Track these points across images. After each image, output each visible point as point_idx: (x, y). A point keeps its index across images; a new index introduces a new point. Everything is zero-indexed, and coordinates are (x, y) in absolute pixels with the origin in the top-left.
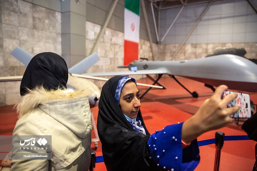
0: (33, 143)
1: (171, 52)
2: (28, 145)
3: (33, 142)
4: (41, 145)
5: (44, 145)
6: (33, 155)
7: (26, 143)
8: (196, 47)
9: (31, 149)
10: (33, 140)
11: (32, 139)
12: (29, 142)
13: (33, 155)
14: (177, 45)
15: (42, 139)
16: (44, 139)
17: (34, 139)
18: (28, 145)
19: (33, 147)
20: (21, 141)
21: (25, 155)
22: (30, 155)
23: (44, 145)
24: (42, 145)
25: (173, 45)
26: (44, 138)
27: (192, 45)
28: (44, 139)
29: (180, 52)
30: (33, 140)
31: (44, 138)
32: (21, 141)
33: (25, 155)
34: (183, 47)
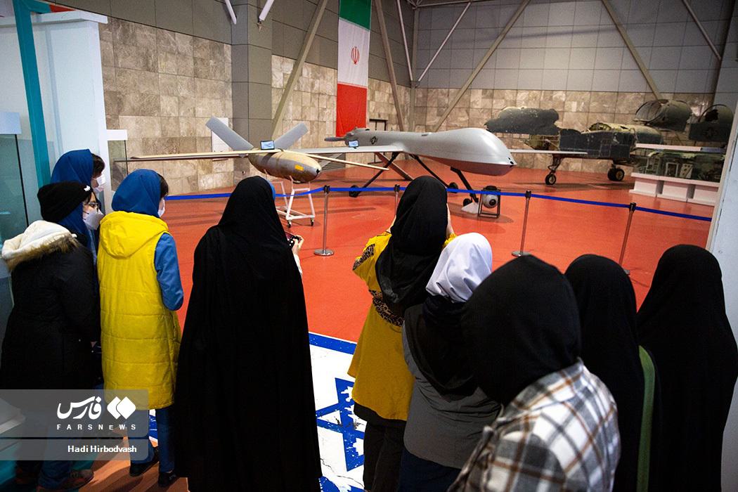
0: (94, 413)
1: (438, 107)
2: (80, 417)
3: (95, 410)
4: (117, 416)
5: (126, 416)
6: (93, 447)
7: (77, 411)
8: (492, 97)
9: (90, 427)
10: (95, 402)
11: (92, 399)
12: (81, 409)
13: (93, 447)
14: (452, 91)
15: (121, 399)
16: (126, 399)
17: (99, 399)
18: (80, 417)
19: (95, 423)
20: (60, 404)
21: (71, 447)
22: (86, 447)
23: (126, 416)
24: (121, 416)
25: (445, 91)
26: (126, 398)
27: (485, 91)
28: (126, 399)
29: (458, 106)
30: (95, 402)
31: (126, 398)
32: (60, 404)
33: (71, 447)
34: (466, 96)
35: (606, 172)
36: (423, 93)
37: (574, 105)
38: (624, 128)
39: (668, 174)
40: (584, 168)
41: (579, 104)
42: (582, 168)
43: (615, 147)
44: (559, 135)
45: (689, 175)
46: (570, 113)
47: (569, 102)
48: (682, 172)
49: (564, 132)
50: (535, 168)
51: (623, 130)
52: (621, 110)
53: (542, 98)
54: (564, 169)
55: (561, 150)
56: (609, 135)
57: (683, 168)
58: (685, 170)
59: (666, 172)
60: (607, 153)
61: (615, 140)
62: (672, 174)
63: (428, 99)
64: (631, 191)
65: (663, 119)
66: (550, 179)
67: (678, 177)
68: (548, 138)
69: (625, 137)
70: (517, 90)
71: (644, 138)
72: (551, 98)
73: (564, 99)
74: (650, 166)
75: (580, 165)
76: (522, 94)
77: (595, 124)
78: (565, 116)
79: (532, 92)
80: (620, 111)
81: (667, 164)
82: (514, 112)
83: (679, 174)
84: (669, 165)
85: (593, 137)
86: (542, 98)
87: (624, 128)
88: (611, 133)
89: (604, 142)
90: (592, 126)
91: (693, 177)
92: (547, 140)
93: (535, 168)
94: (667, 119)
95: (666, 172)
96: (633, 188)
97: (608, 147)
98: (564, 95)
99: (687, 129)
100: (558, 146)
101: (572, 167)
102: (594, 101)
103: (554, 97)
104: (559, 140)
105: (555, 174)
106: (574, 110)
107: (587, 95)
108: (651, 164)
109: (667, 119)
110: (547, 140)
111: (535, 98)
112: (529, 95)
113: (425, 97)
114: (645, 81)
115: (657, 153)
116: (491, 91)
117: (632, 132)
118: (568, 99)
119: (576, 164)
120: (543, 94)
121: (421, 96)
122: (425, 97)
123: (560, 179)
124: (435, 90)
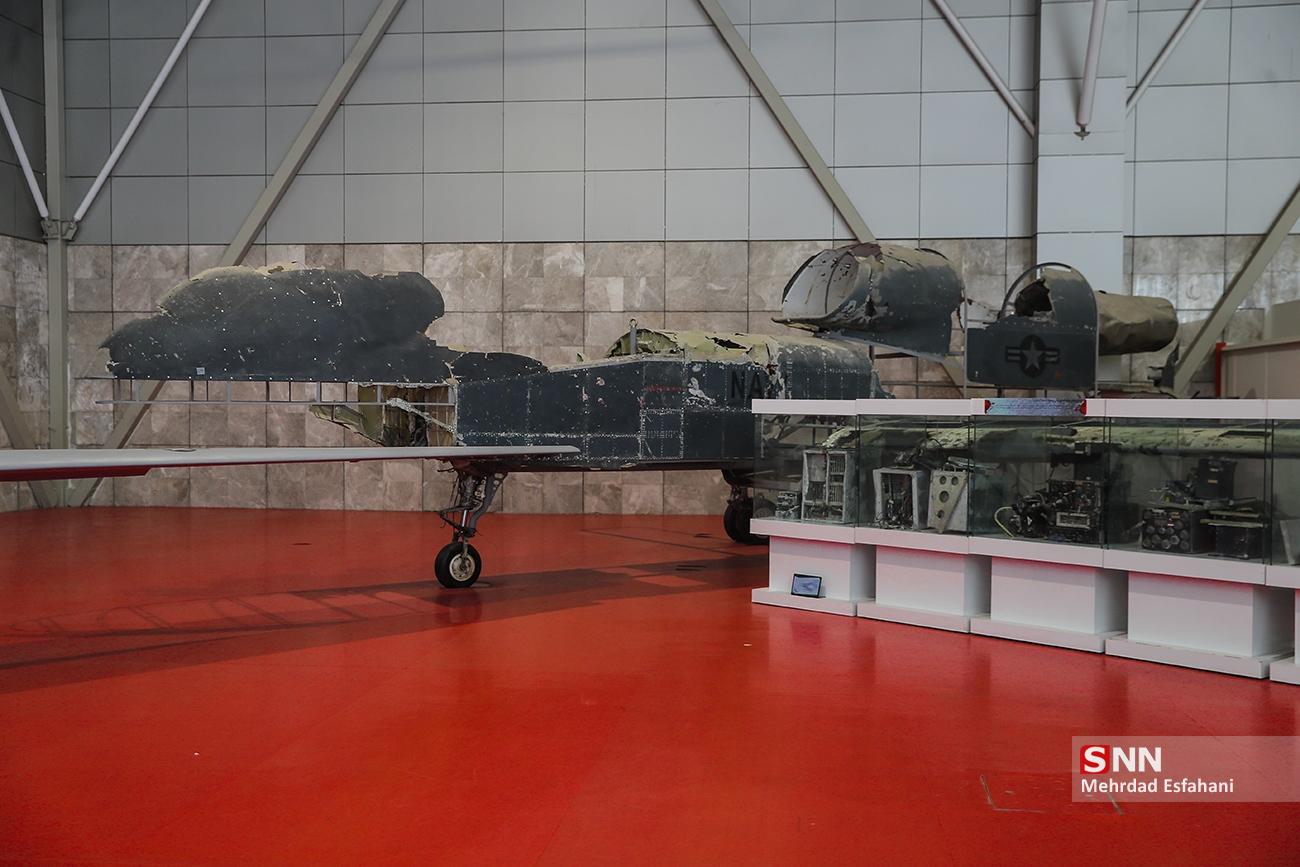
25: (175, 254)
35: (722, 509)
36: (95, 263)
37: (616, 288)
38: (728, 344)
39: (886, 518)
40: (671, 500)
41: (630, 285)
42: (665, 501)
43: (700, 425)
44: (453, 381)
45: (960, 520)
46: (605, 317)
47: (599, 280)
48: (934, 506)
49: (470, 365)
50: (506, 511)
51: (724, 357)
52: (766, 296)
53: (508, 269)
54: (605, 509)
55: (469, 442)
56: (666, 379)
57: (936, 488)
58: (944, 495)
59: (879, 508)
60: (672, 446)
61: (696, 391)
62: (899, 516)
63: (117, 284)
64: (758, 595)
65: (871, 310)
66: (455, 563)
67: (924, 526)
68: (403, 394)
69: (734, 373)
70: (423, 244)
71: (808, 378)
72: (538, 270)
73: (579, 270)
74: (816, 489)
75: (658, 489)
76: (441, 258)
77: (627, 336)
78: (589, 329)
79: (473, 251)
80: (761, 301)
81: (877, 474)
82: (231, 288)
83: (924, 516)
84: (886, 478)
85: (601, 382)
86: (508, 269)
87: (728, 344)
88: (679, 366)
89: (654, 400)
90: (619, 344)
91: (979, 525)
92: (398, 402)
93: (506, 511)
94: (881, 311)
95: (879, 508)
96: (764, 582)
97: (671, 422)
98: (580, 255)
99: (958, 342)
100: (452, 426)
101: (632, 499)
102: (678, 274)
103: (547, 263)
104: (453, 398)
105: (470, 541)
106: (617, 305)
107: (652, 255)
108: (817, 478)
109: (881, 311)
110: (398, 402)
111: (487, 269)
112: (464, 258)
113: (105, 275)
114: (829, 210)
115: (854, 435)
116: (337, 250)
117: (762, 359)
118: (595, 268)
119: (645, 489)
120: (509, 258)
121: (87, 273)
122: (105, 275)
123: (510, 557)
124: (137, 252)
